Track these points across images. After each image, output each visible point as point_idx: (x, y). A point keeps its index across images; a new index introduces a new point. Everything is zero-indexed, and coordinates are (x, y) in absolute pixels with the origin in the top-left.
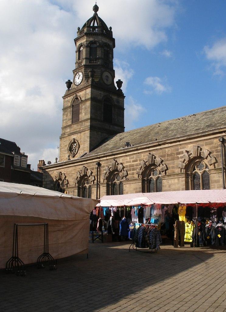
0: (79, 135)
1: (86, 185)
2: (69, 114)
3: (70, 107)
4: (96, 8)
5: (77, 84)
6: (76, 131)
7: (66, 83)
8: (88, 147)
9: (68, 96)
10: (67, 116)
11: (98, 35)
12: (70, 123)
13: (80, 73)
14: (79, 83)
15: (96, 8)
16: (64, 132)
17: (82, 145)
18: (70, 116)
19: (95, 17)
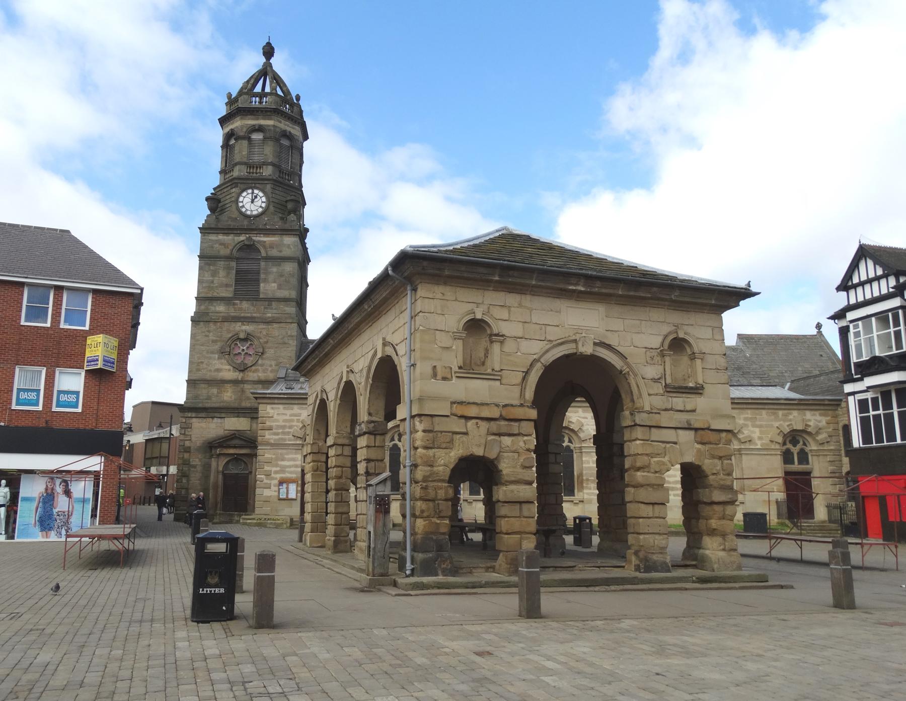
0: (262, 326)
1: (396, 442)
2: (222, 273)
3: (229, 258)
4: (269, 51)
5: (249, 213)
6: (249, 315)
7: (207, 199)
8: (291, 357)
9: (223, 232)
10: (214, 274)
11: (295, 122)
12: (228, 293)
13: (256, 191)
14: (255, 213)
15: (269, 51)
16: (203, 307)
17: (272, 351)
18: (224, 277)
19: (266, 72)
